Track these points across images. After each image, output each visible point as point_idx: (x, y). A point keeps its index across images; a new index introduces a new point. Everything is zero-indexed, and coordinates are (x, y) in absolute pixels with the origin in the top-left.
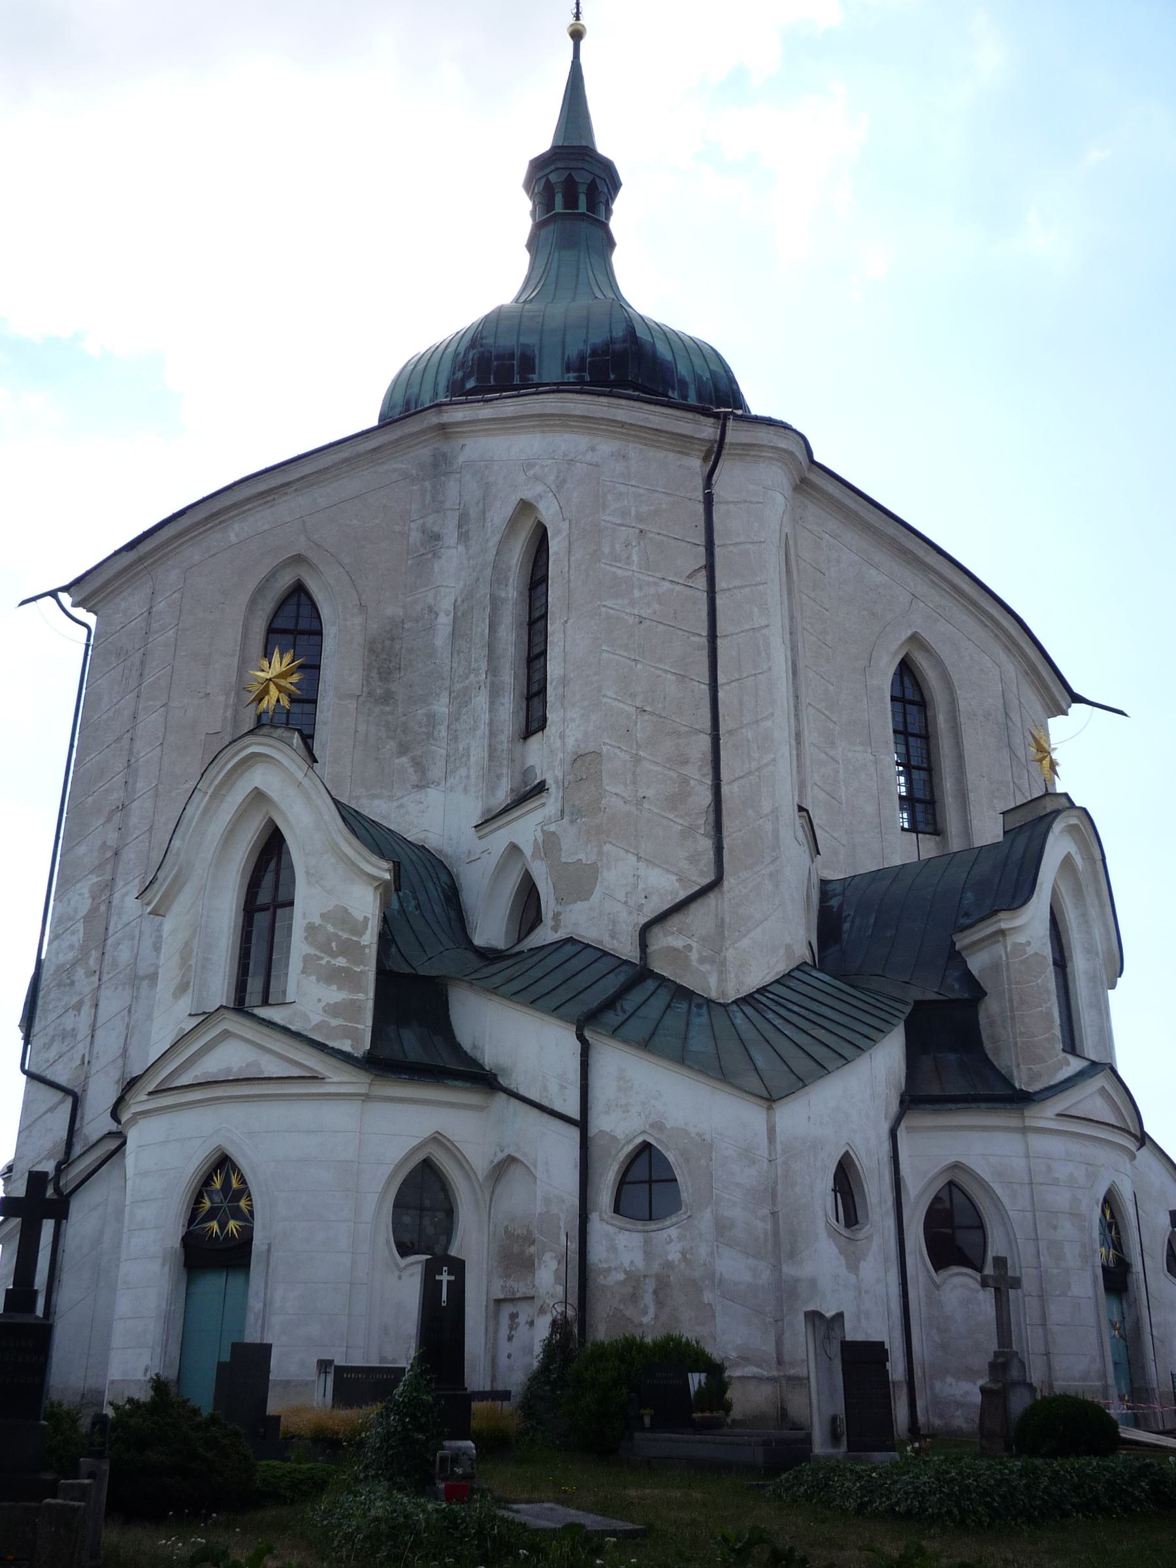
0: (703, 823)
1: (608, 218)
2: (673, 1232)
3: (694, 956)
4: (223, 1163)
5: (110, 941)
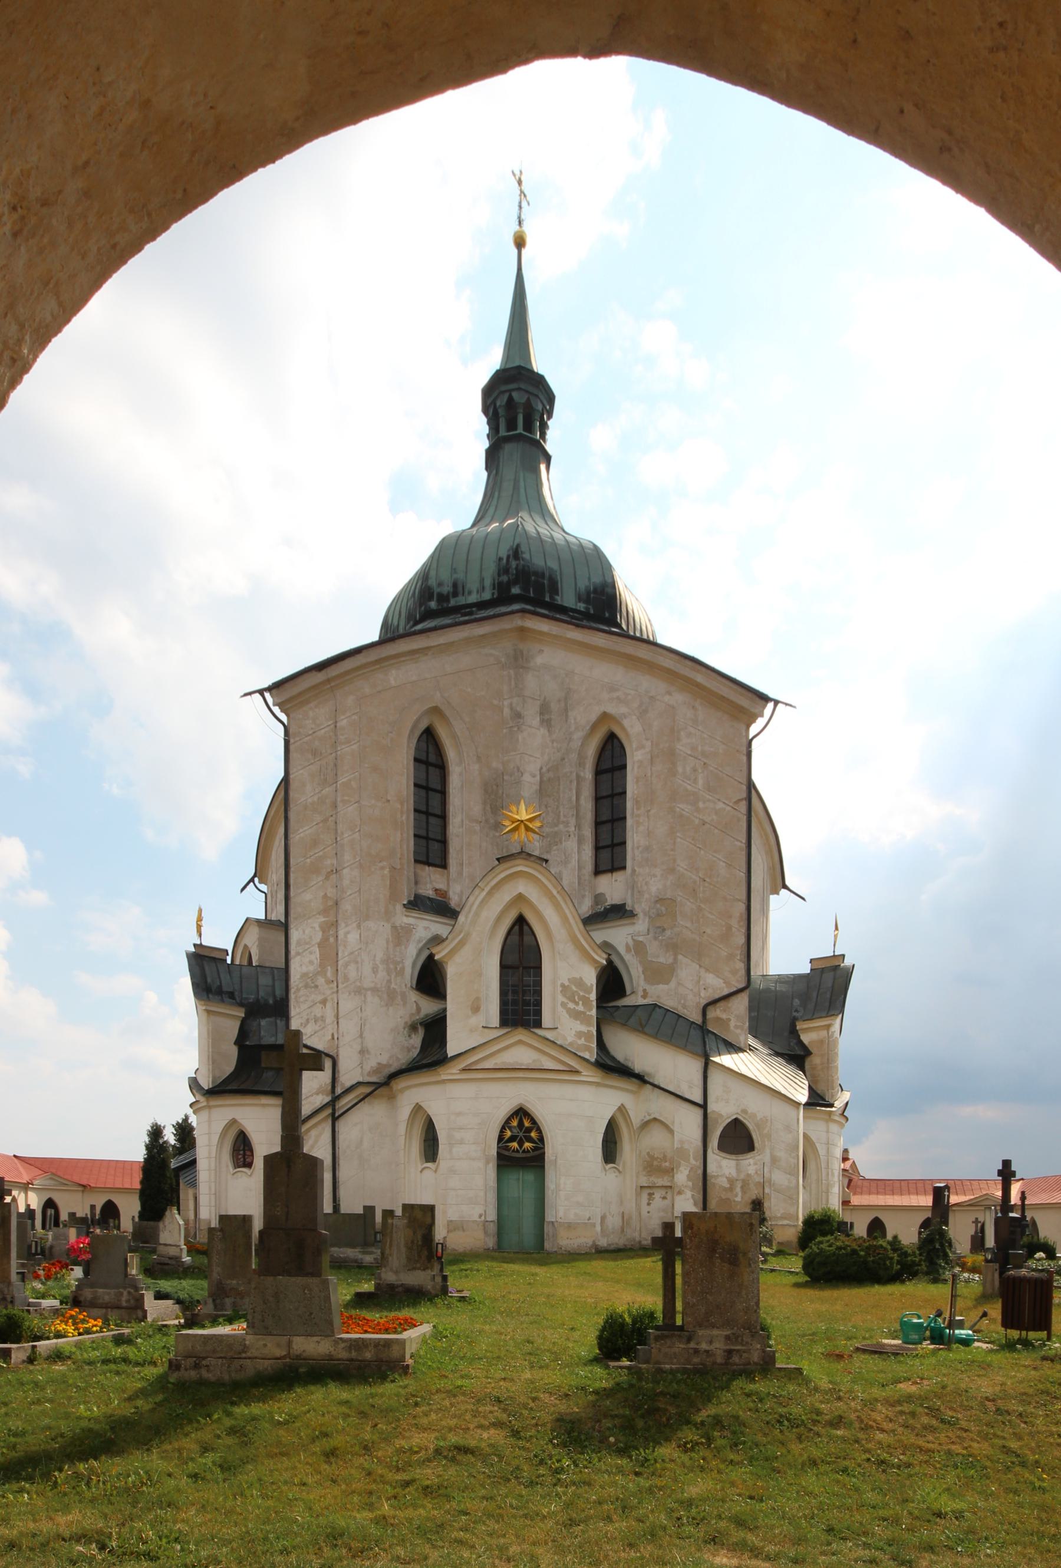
0: (739, 954)
1: (543, 435)
2: (751, 1161)
3: (732, 1024)
4: (521, 1113)
5: (340, 963)
